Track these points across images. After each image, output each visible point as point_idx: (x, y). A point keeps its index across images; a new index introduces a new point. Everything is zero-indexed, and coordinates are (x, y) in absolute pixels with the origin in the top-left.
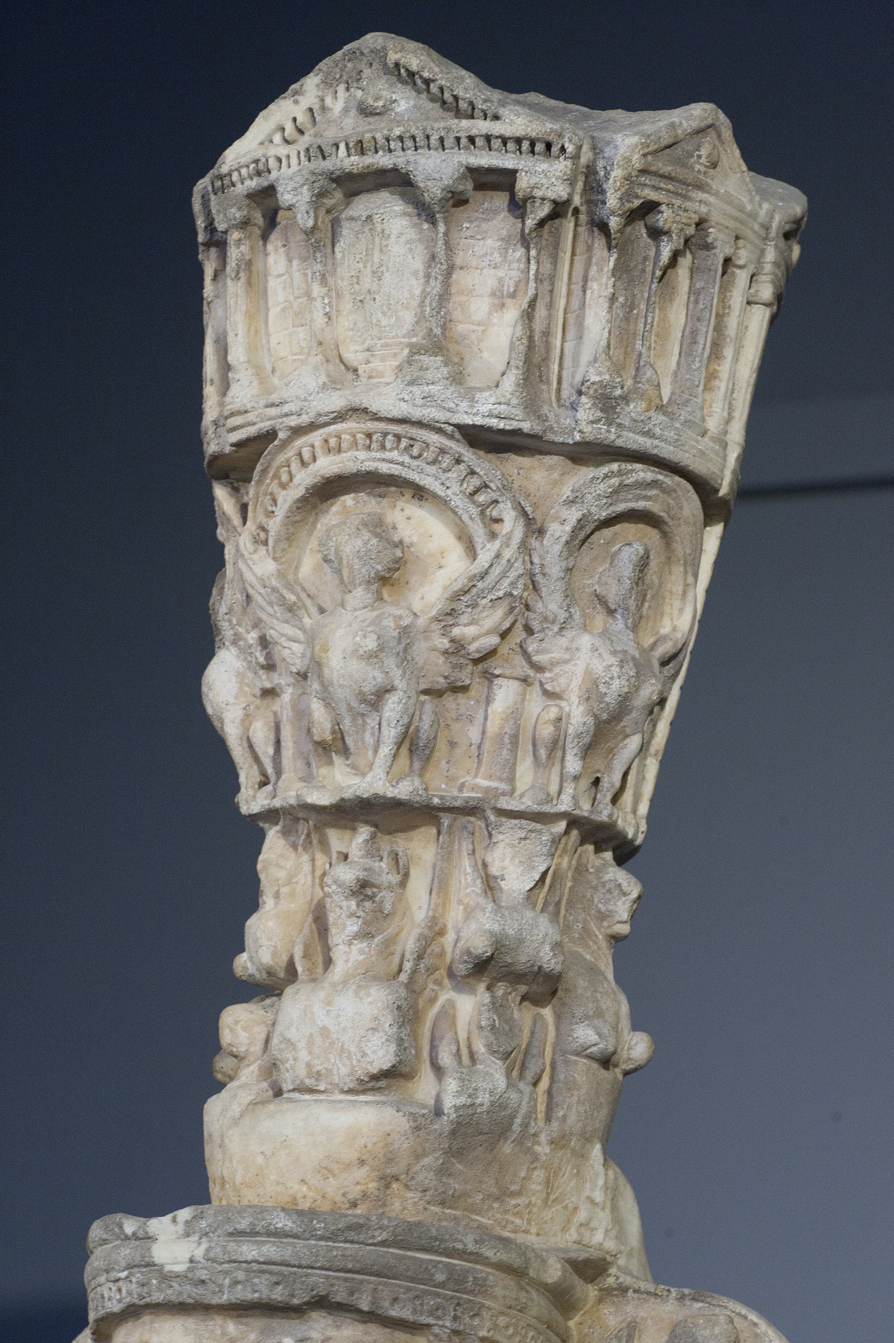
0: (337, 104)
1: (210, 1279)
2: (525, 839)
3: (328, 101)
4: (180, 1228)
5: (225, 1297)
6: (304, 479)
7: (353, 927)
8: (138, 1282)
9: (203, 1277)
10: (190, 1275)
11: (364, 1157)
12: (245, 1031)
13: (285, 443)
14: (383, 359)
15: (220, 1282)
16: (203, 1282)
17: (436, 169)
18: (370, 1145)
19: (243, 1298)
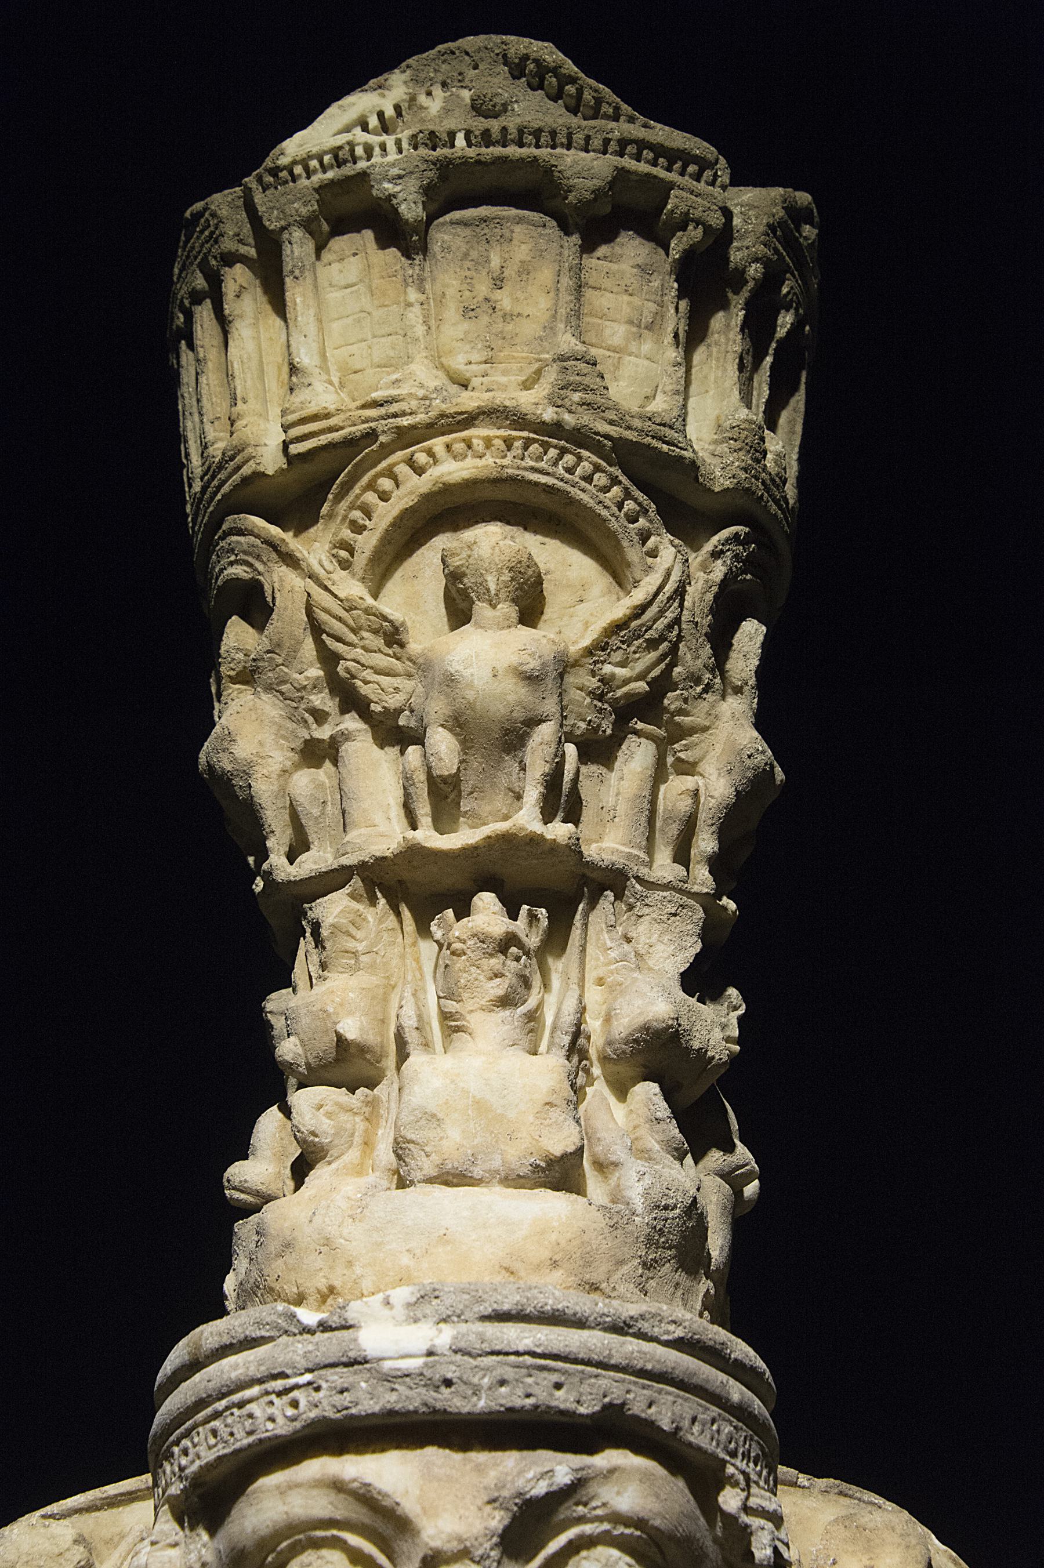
0: (434, 104)
1: (460, 1378)
2: (675, 915)
3: (422, 99)
4: (399, 1311)
5: (482, 1404)
6: (411, 489)
7: (497, 988)
8: (331, 1389)
9: (449, 1375)
10: (428, 1373)
11: (556, 1257)
12: (329, 1118)
13: (387, 450)
14: (505, 373)
15: (475, 1380)
16: (448, 1383)
17: (584, 169)
18: (563, 1243)
19: (509, 1405)
